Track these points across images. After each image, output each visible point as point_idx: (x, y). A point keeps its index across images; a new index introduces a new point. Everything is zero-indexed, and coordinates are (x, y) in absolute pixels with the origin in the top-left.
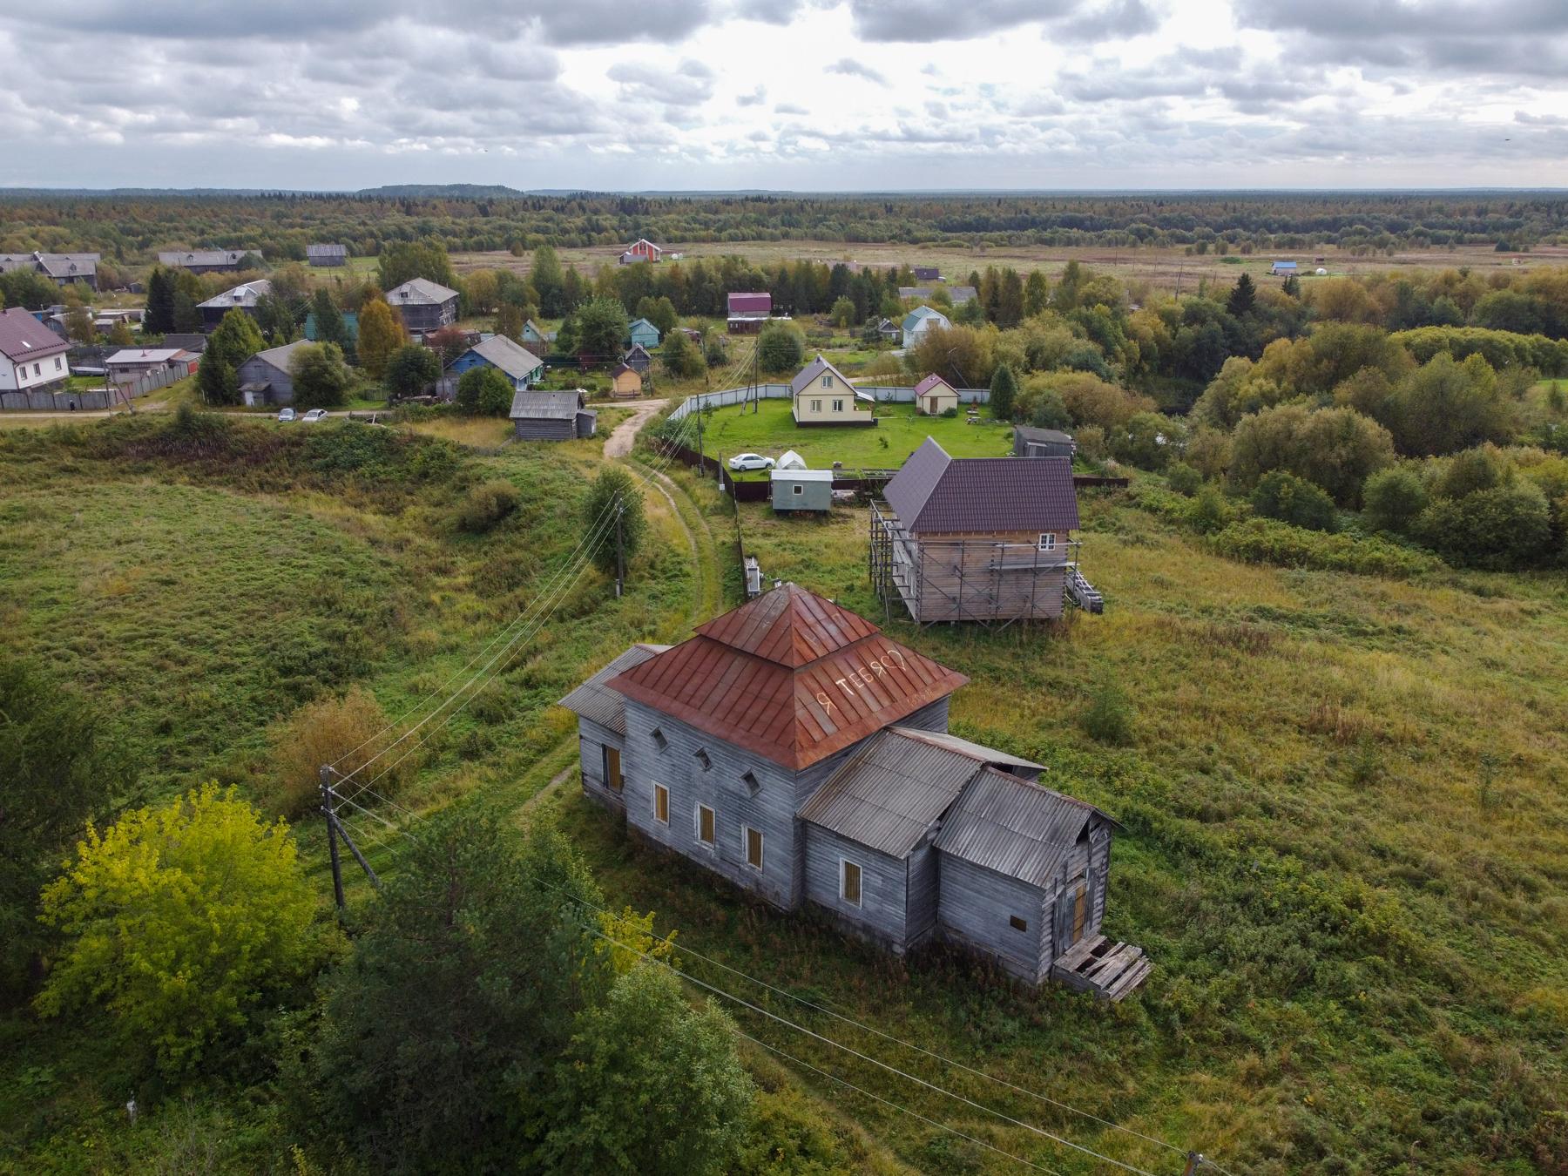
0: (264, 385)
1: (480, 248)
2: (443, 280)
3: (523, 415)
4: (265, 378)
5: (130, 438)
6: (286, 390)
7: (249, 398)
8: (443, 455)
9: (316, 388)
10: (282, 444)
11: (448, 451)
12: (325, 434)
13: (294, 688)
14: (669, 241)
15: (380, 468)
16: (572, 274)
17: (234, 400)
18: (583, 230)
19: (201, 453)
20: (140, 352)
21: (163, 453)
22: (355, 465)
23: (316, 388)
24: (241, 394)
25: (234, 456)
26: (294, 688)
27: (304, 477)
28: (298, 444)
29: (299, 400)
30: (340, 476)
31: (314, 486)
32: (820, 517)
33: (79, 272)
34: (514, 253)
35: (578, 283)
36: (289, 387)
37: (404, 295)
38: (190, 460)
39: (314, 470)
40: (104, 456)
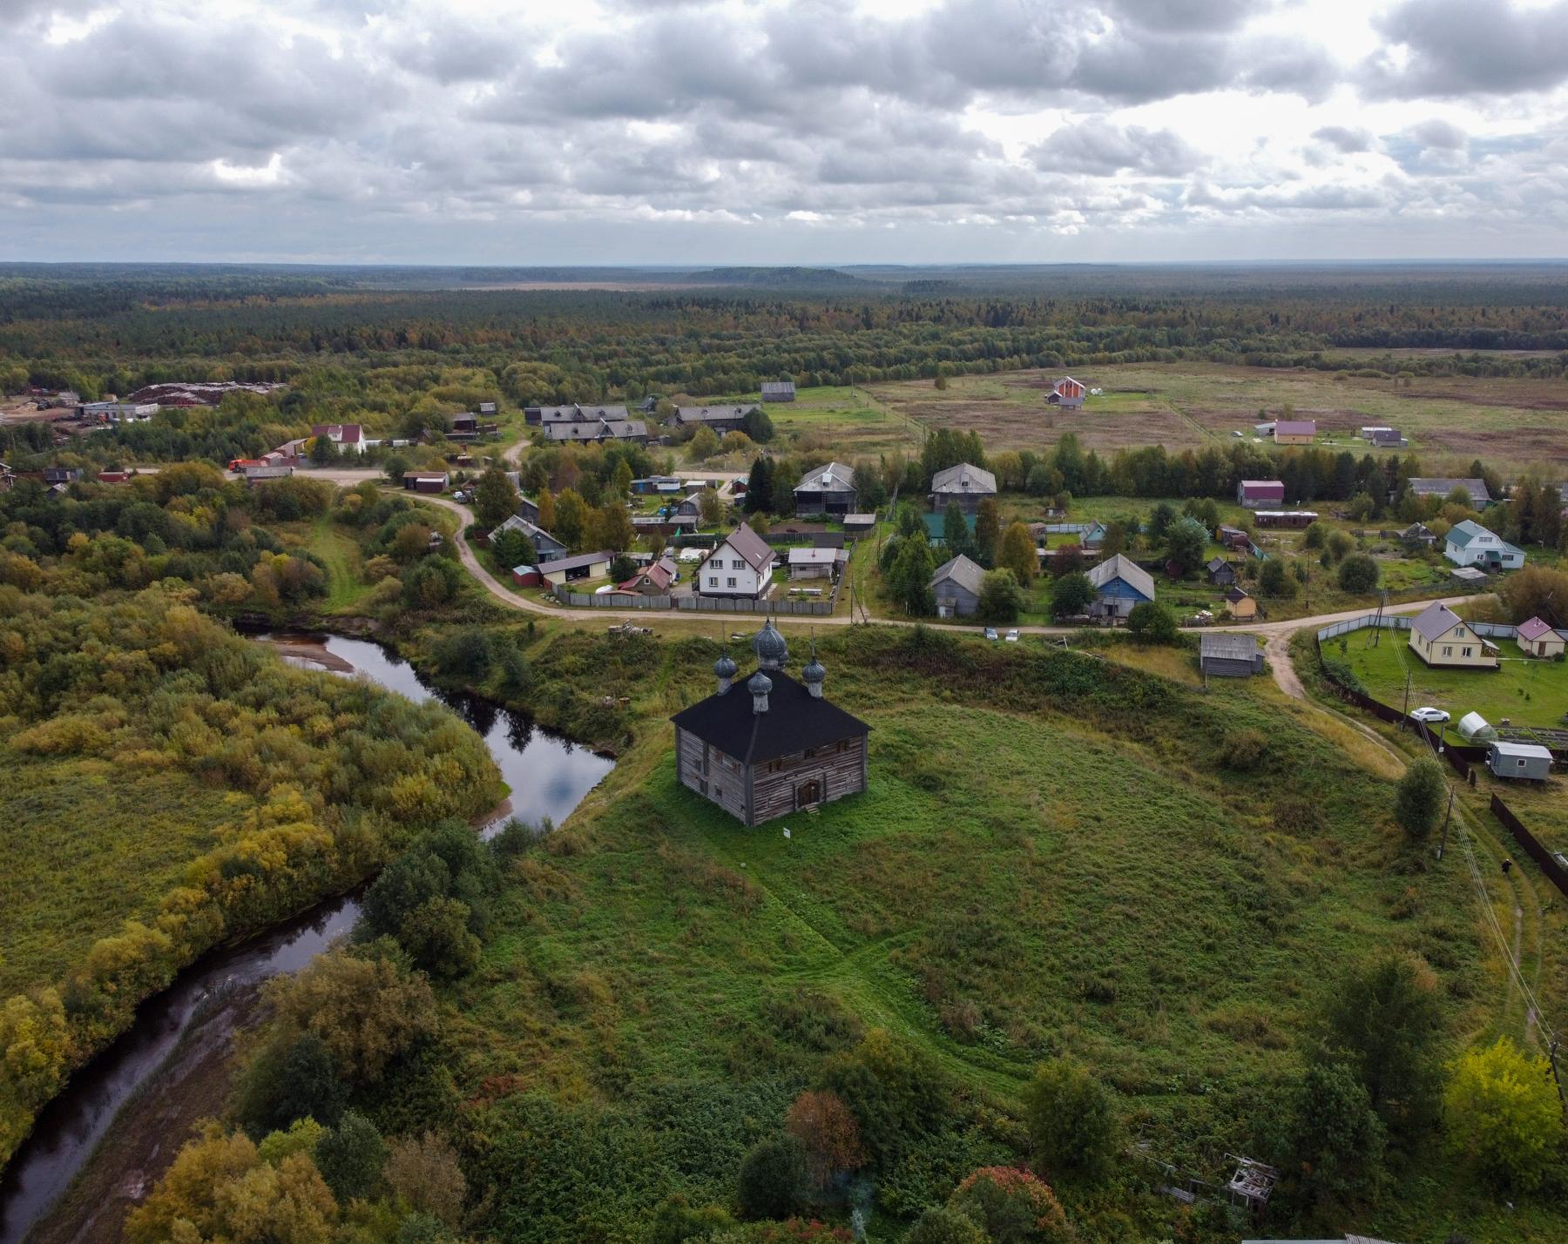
0: (953, 601)
1: (898, 377)
2: (979, 463)
3: (1212, 655)
4: (951, 595)
5: (875, 647)
6: (969, 607)
7: (942, 611)
8: (1162, 691)
9: (997, 608)
10: (1009, 664)
11: (1165, 686)
12: (1044, 658)
13: (1263, 920)
14: (1068, 364)
15: (1104, 694)
16: (1092, 458)
17: (932, 614)
18: (981, 354)
19: (945, 667)
20: (810, 551)
21: (910, 665)
22: (1082, 691)
23: (997, 608)
24: (936, 608)
25: (971, 673)
26: (1263, 920)
27: (1042, 698)
28: (1020, 665)
29: (987, 615)
30: (1074, 700)
31: (1057, 708)
32: (1538, 785)
33: (634, 433)
34: (939, 386)
35: (1097, 467)
36: (974, 603)
37: (965, 484)
38: (935, 673)
39: (1047, 693)
40: (864, 663)
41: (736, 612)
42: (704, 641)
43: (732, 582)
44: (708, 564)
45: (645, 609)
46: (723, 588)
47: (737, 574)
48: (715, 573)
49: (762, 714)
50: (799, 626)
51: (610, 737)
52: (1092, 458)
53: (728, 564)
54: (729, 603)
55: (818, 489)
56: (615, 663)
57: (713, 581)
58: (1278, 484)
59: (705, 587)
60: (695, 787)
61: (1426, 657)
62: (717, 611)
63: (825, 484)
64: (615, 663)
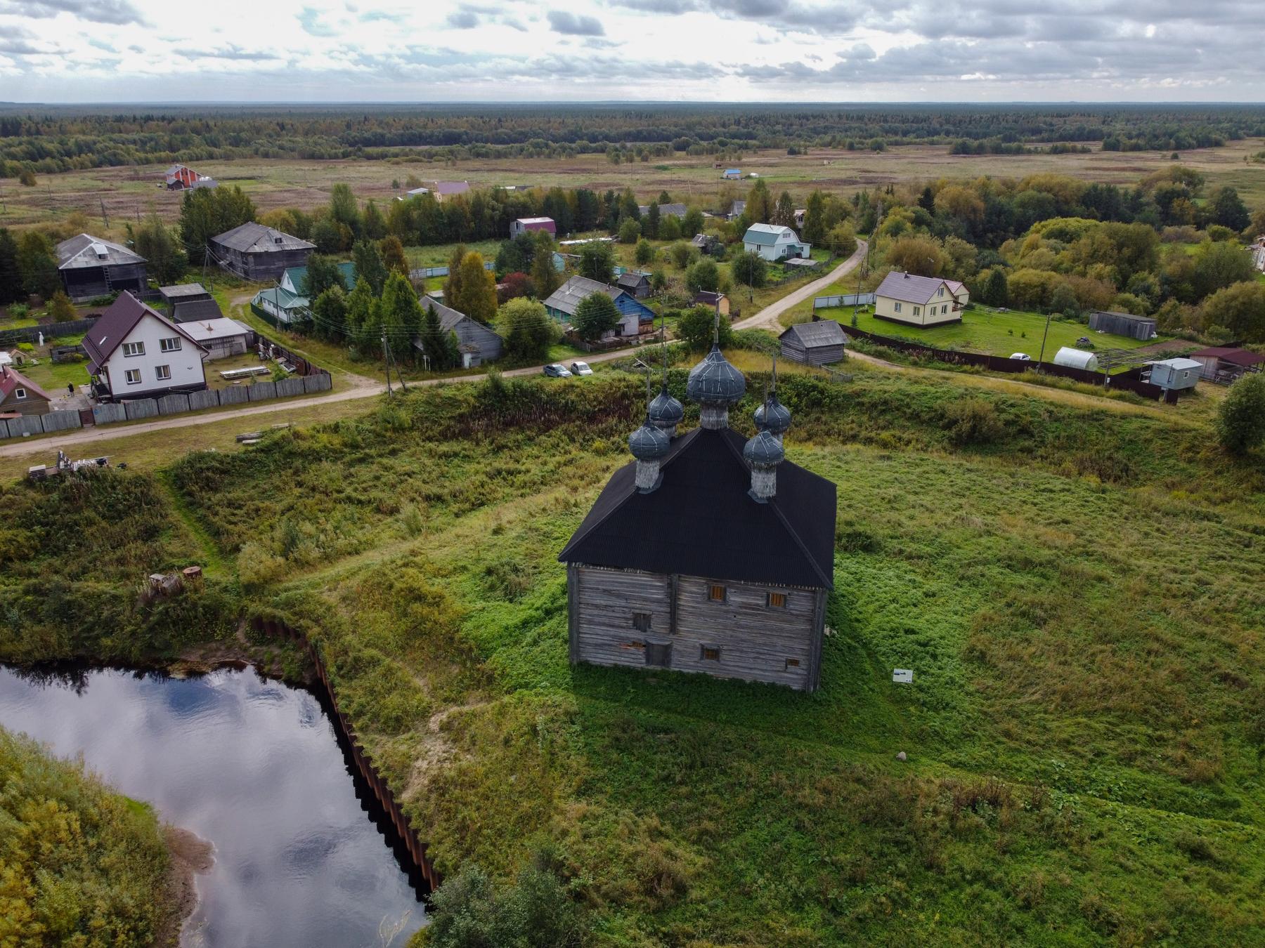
7: (467, 359)
16: (371, 208)
41: (192, 412)
42: (213, 457)
43: (162, 371)
44: (120, 350)
45: (35, 436)
46: (150, 382)
47: (168, 358)
48: (133, 363)
49: (751, 502)
50: (276, 415)
51: (208, 638)
52: (371, 208)
53: (153, 347)
54: (180, 401)
55: (94, 263)
56: (90, 523)
57: (132, 376)
58: (548, 220)
59: (119, 386)
60: (634, 659)
61: (918, 320)
62: (162, 416)
63: (101, 257)
64: (90, 523)
